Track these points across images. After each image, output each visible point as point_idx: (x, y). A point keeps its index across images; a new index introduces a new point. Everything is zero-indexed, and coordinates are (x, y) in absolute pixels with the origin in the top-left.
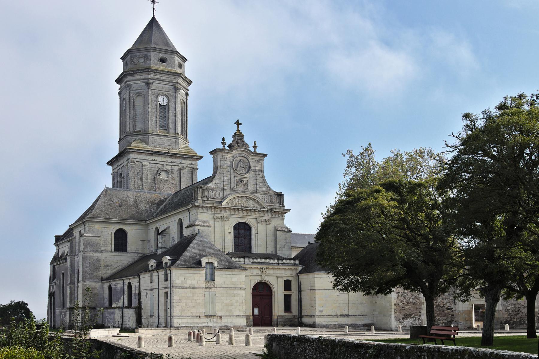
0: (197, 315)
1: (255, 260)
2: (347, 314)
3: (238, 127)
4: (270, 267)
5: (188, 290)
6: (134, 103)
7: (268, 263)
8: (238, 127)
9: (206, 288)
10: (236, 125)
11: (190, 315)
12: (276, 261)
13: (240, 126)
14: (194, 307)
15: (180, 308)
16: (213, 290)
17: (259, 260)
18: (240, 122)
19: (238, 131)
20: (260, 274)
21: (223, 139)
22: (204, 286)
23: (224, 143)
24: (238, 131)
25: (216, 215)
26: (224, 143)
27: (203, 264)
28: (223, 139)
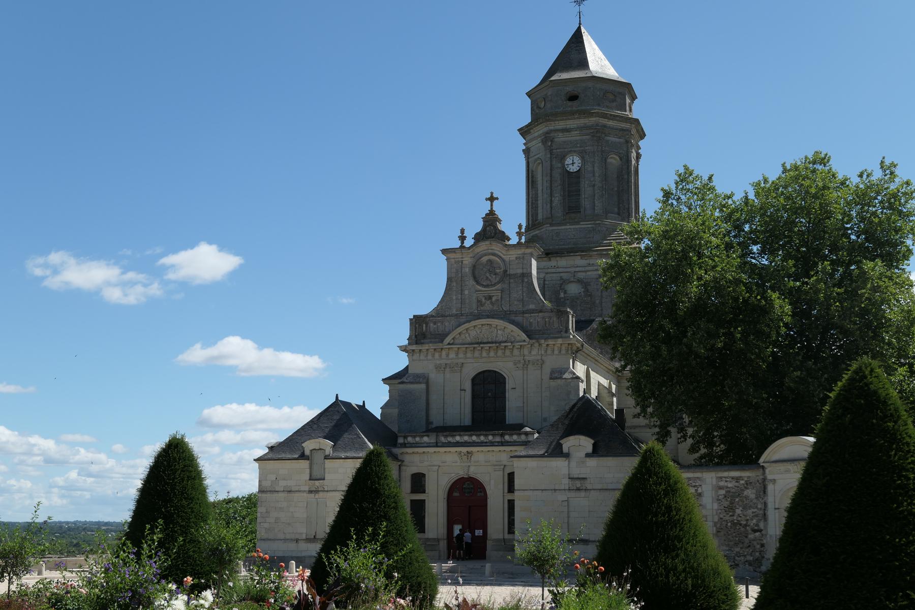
0: (293, 537)
1: (450, 439)
2: (587, 537)
3: (492, 205)
4: (474, 449)
5: (281, 495)
6: (533, 177)
7: (474, 442)
8: (492, 205)
9: (310, 492)
10: (489, 202)
11: (282, 537)
12: (490, 438)
13: (495, 202)
14: (289, 524)
15: (266, 525)
16: (321, 494)
17: (458, 438)
18: (495, 196)
19: (492, 212)
20: (458, 464)
21: (462, 231)
22: (307, 488)
23: (463, 238)
24: (492, 212)
25: (438, 362)
26: (463, 238)
27: (307, 452)
28: (462, 231)
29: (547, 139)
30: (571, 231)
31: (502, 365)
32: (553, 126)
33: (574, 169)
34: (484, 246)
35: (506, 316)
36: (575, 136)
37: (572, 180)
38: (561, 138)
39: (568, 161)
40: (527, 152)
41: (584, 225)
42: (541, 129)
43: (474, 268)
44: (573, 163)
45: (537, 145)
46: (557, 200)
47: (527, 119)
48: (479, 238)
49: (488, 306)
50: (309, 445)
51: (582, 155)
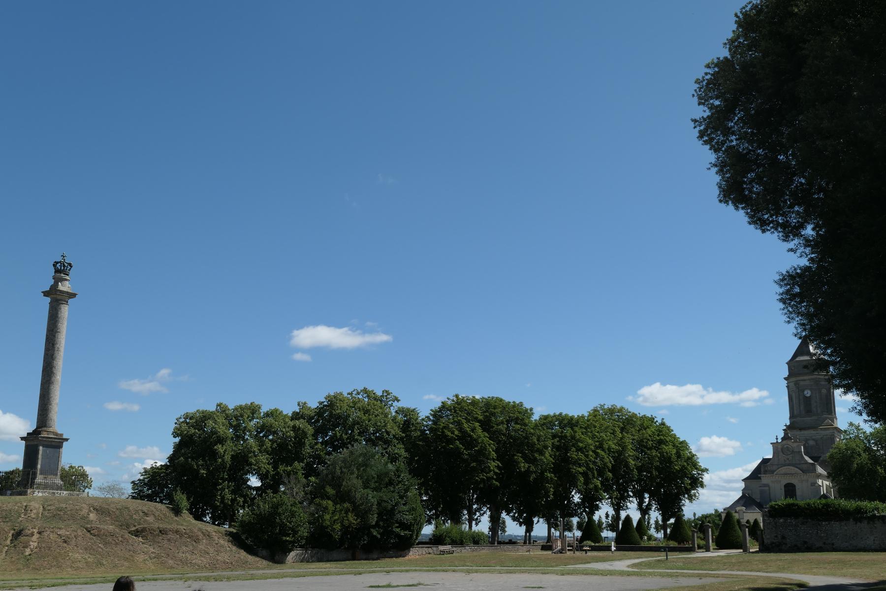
29: (796, 383)
30: (808, 420)
31: (794, 481)
32: (798, 378)
33: (808, 395)
34: (785, 442)
35: (795, 465)
36: (807, 383)
37: (807, 400)
38: (802, 383)
39: (806, 392)
40: (788, 387)
41: (814, 418)
42: (794, 379)
43: (782, 449)
44: (808, 393)
45: (792, 385)
46: (802, 407)
47: (786, 374)
48: (783, 439)
49: (787, 462)
50: (738, 509)
51: (811, 389)
